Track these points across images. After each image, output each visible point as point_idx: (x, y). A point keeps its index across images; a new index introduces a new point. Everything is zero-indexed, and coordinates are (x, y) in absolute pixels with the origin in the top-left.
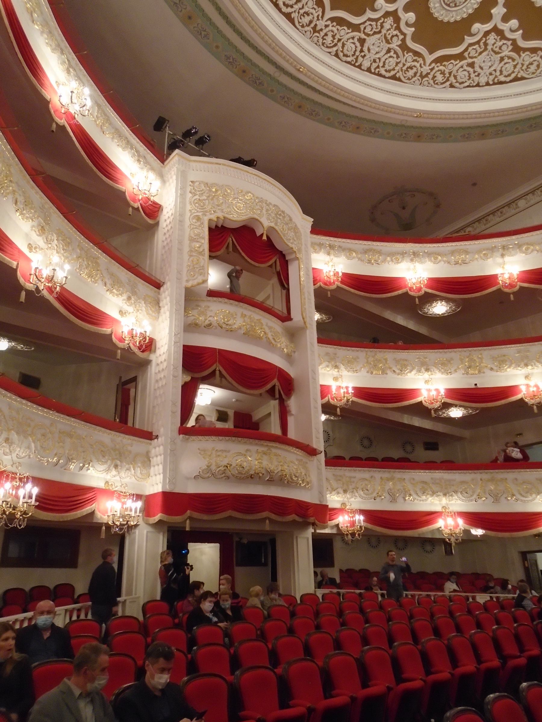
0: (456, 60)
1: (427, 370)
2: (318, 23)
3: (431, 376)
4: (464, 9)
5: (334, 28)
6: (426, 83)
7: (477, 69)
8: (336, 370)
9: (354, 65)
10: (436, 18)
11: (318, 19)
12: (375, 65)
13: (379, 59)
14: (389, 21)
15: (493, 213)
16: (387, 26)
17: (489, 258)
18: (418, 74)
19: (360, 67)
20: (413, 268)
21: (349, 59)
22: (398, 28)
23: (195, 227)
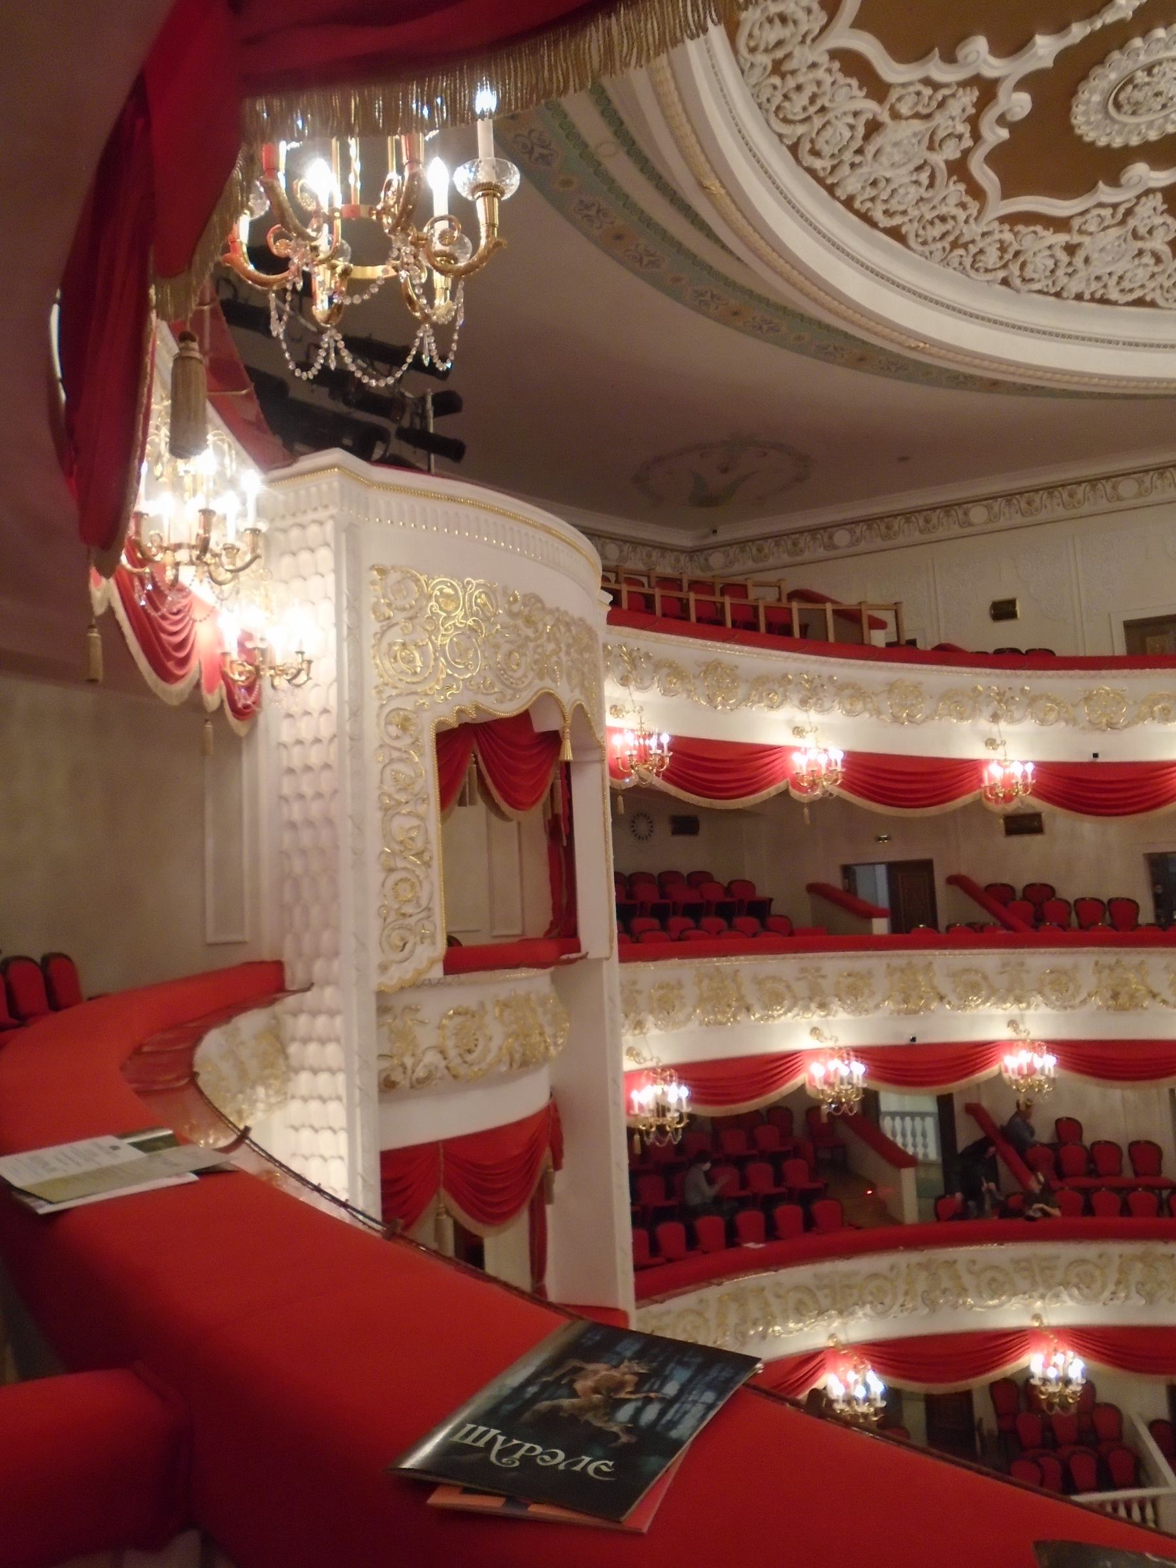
0: (1046, 228)
1: (822, 1006)
2: (797, 52)
3: (830, 1018)
4: (1143, 127)
5: (828, 75)
6: (955, 262)
7: (1078, 260)
8: (637, 1032)
9: (820, 181)
10: (1093, 143)
11: (803, 42)
12: (870, 192)
13: (888, 180)
14: (968, 98)
15: (908, 515)
16: (954, 107)
17: (967, 719)
18: (951, 238)
19: (831, 189)
20: (809, 731)
21: (818, 164)
22: (974, 122)
23: (396, 754)
